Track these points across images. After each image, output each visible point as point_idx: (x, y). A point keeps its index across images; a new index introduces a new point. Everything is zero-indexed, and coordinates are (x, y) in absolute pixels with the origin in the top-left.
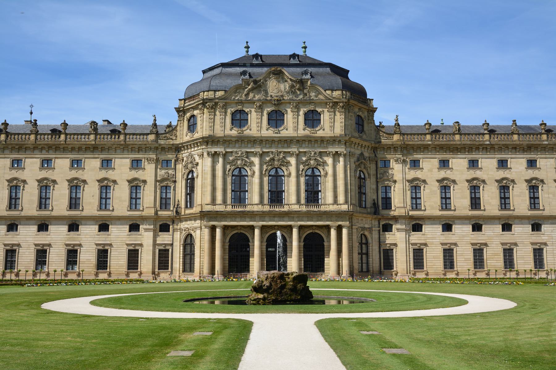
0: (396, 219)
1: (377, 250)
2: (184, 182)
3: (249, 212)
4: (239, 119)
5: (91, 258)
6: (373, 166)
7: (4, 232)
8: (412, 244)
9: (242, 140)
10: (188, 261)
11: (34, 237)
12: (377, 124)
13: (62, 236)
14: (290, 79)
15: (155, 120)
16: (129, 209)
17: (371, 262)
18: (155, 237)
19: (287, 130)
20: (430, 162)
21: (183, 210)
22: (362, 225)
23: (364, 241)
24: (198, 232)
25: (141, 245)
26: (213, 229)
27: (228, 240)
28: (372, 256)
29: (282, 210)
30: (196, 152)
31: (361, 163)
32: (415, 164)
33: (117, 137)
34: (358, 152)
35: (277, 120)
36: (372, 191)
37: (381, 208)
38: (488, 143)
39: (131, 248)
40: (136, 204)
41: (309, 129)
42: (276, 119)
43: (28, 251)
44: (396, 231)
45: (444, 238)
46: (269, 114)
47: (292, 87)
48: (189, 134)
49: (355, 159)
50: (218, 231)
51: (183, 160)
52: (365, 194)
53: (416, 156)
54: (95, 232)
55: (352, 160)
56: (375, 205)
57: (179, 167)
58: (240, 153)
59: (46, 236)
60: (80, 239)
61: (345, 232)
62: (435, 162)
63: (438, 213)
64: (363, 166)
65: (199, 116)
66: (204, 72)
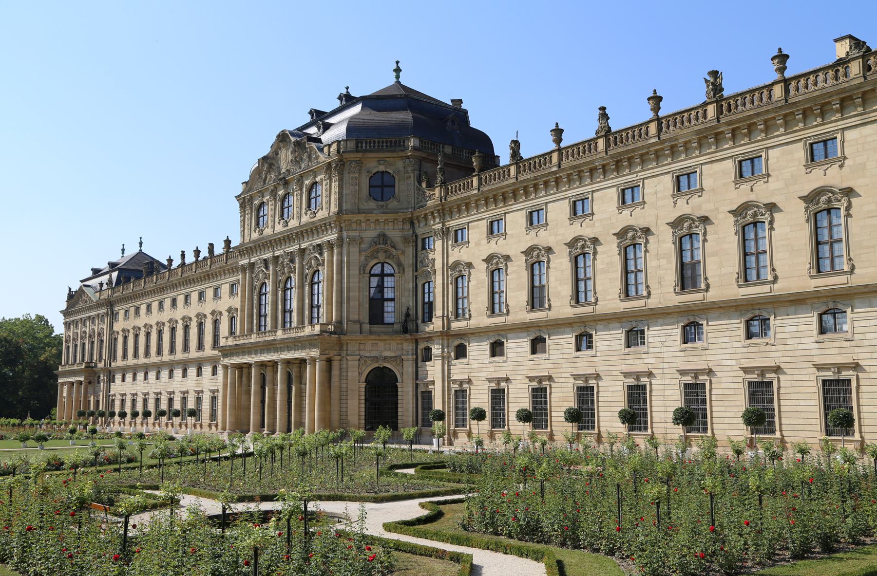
6: (410, 251)
20: (477, 227)
22: (374, 354)
34: (370, 234)
37: (420, 321)
63: (487, 322)
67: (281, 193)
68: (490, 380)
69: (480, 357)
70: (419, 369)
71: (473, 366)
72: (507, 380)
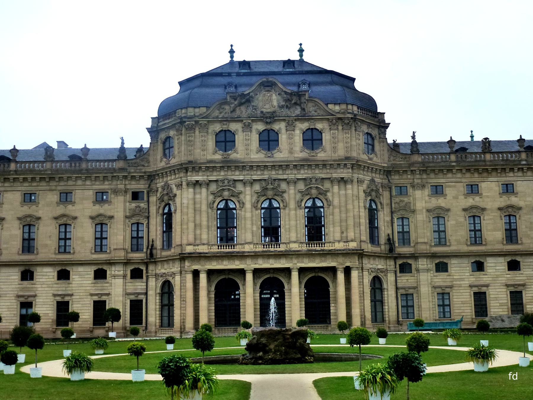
0: (415, 257)
1: (394, 295)
2: (159, 218)
3: (238, 252)
4: (225, 141)
5: (48, 312)
6: (386, 194)
8: (435, 287)
9: (228, 165)
10: (166, 314)
12: (390, 141)
13: (14, 286)
14: (285, 92)
15: (123, 143)
16: (93, 251)
17: (387, 310)
18: (125, 284)
19: (281, 152)
20: (455, 186)
21: (159, 252)
22: (374, 266)
23: (377, 286)
24: (178, 278)
25: (108, 294)
26: (196, 274)
27: (213, 288)
28: (388, 303)
29: (278, 249)
30: (172, 181)
31: (372, 190)
32: (438, 190)
33: (77, 165)
35: (269, 141)
36: (386, 224)
37: (397, 245)
38: (524, 162)
39: (96, 298)
40: (101, 245)
41: (308, 152)
42: (269, 141)
44: (416, 272)
45: (474, 279)
46: (260, 134)
47: (286, 101)
48: (165, 160)
49: (365, 186)
50: (203, 277)
51: (157, 191)
52: (377, 228)
53: (441, 180)
54: (53, 280)
55: (361, 189)
56: (390, 241)
57: (153, 199)
58: (226, 182)
60: (35, 289)
61: (355, 274)
62: (461, 188)
63: (465, 249)
64: (374, 194)
65: (176, 137)
66: (181, 83)
67: (261, 127)
68: (471, 286)
69: (462, 271)
70: (398, 278)
71: (455, 277)
72: (487, 286)
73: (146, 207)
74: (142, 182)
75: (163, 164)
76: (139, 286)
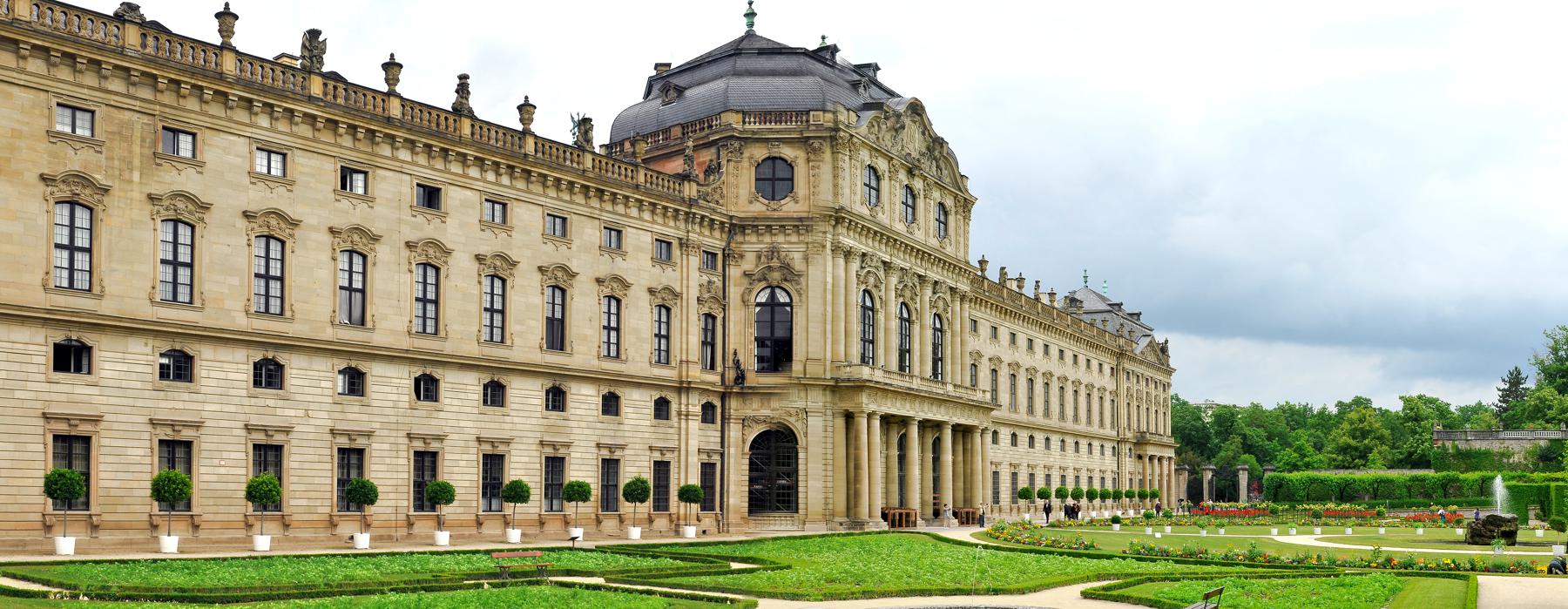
7: (406, 398)
11: (471, 417)
13: (534, 421)
30: (792, 248)
39: (657, 456)
43: (465, 457)
51: (742, 256)
57: (734, 272)
59: (501, 419)
73: (720, 284)
74: (717, 234)
75: (759, 208)
76: (713, 433)
